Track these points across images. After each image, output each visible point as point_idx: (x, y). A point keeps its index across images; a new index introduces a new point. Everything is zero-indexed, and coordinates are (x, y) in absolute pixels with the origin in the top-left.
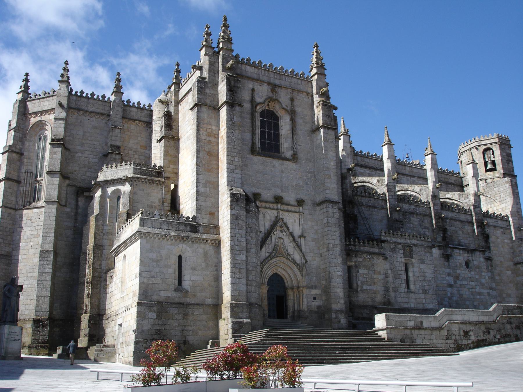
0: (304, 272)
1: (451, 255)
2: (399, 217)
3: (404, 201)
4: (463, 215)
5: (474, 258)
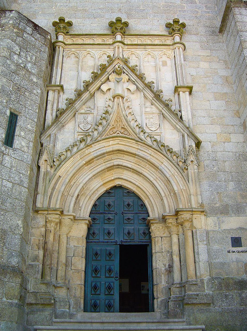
0: (192, 169)
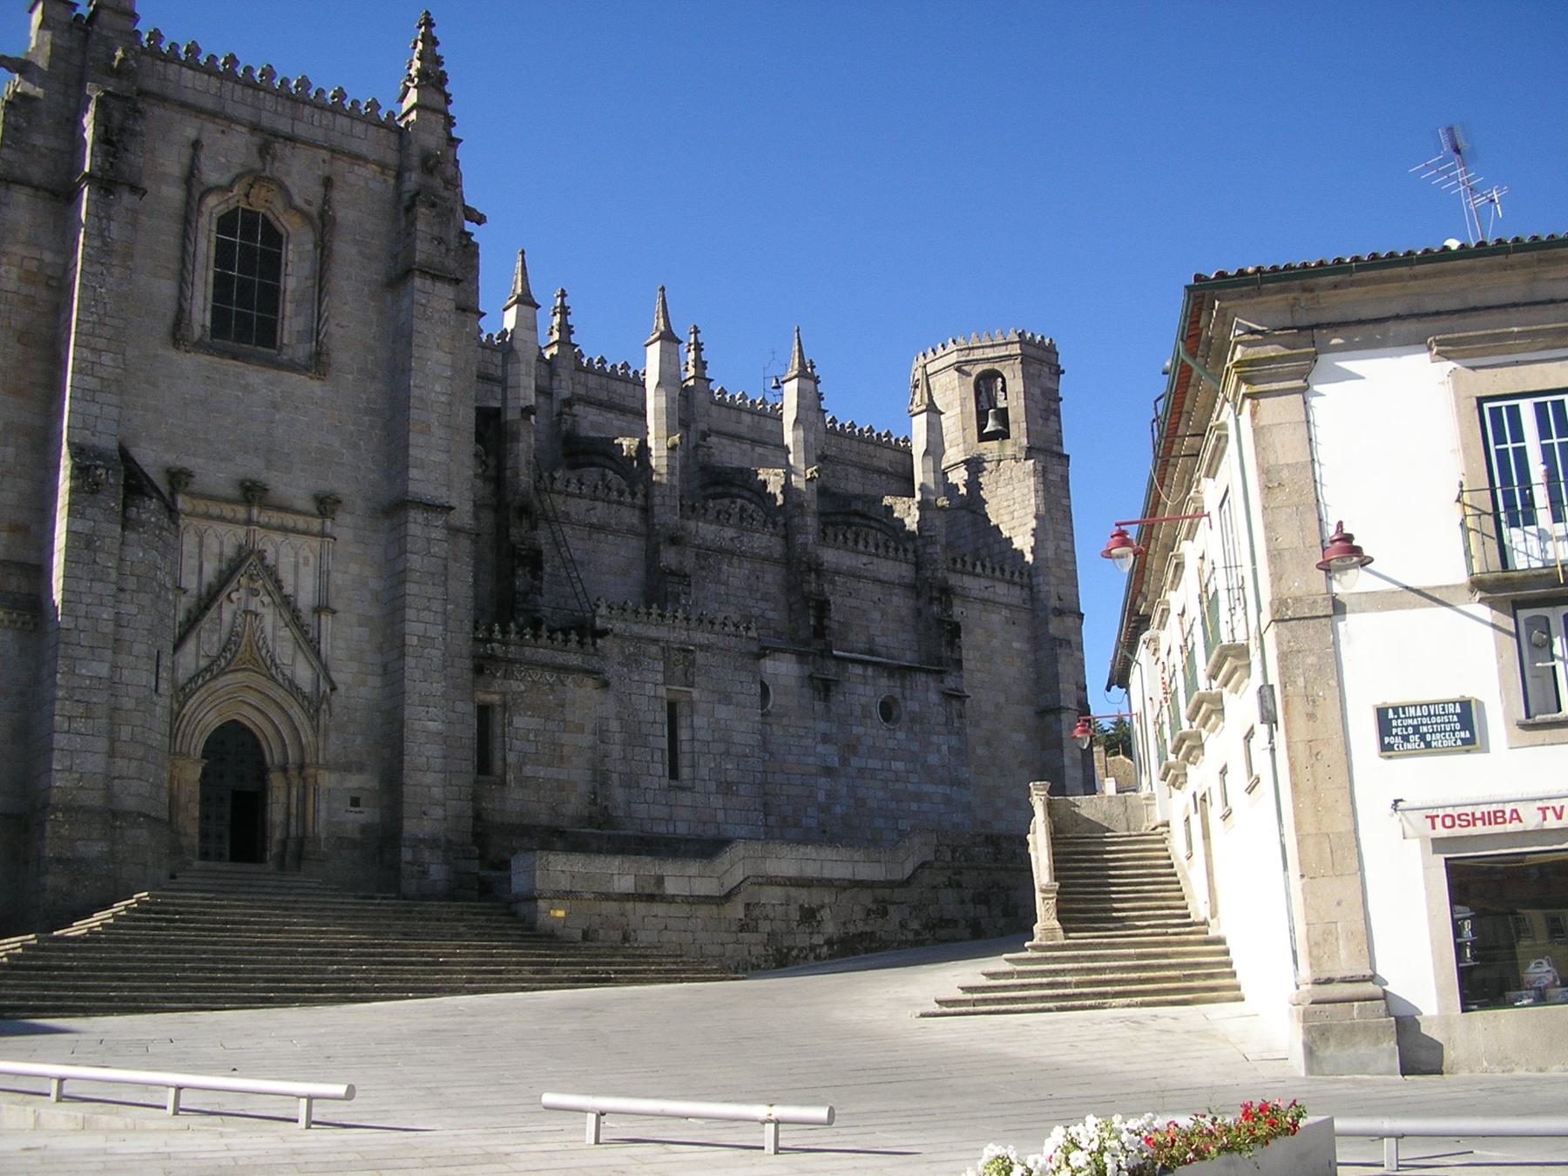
1: (837, 682)
2: (681, 563)
3: (704, 514)
4: (890, 563)
5: (908, 693)
